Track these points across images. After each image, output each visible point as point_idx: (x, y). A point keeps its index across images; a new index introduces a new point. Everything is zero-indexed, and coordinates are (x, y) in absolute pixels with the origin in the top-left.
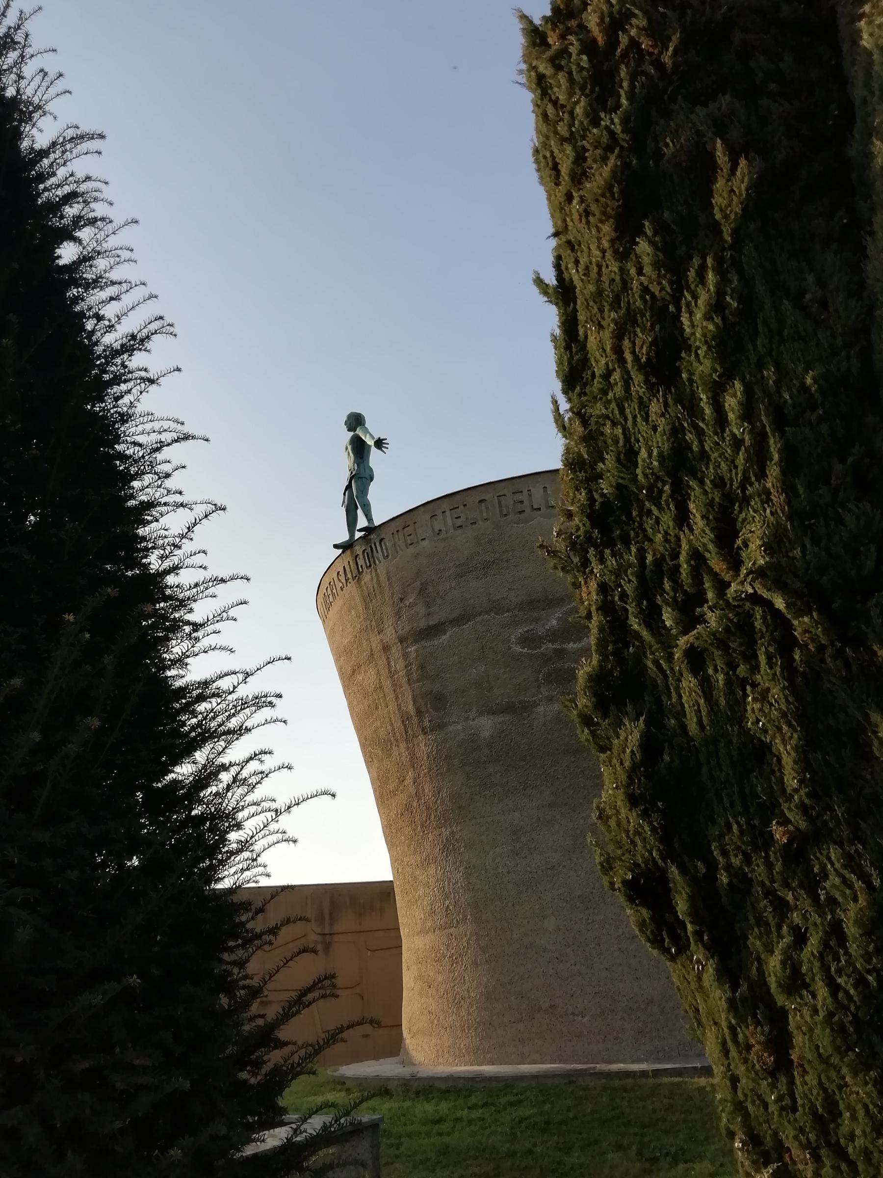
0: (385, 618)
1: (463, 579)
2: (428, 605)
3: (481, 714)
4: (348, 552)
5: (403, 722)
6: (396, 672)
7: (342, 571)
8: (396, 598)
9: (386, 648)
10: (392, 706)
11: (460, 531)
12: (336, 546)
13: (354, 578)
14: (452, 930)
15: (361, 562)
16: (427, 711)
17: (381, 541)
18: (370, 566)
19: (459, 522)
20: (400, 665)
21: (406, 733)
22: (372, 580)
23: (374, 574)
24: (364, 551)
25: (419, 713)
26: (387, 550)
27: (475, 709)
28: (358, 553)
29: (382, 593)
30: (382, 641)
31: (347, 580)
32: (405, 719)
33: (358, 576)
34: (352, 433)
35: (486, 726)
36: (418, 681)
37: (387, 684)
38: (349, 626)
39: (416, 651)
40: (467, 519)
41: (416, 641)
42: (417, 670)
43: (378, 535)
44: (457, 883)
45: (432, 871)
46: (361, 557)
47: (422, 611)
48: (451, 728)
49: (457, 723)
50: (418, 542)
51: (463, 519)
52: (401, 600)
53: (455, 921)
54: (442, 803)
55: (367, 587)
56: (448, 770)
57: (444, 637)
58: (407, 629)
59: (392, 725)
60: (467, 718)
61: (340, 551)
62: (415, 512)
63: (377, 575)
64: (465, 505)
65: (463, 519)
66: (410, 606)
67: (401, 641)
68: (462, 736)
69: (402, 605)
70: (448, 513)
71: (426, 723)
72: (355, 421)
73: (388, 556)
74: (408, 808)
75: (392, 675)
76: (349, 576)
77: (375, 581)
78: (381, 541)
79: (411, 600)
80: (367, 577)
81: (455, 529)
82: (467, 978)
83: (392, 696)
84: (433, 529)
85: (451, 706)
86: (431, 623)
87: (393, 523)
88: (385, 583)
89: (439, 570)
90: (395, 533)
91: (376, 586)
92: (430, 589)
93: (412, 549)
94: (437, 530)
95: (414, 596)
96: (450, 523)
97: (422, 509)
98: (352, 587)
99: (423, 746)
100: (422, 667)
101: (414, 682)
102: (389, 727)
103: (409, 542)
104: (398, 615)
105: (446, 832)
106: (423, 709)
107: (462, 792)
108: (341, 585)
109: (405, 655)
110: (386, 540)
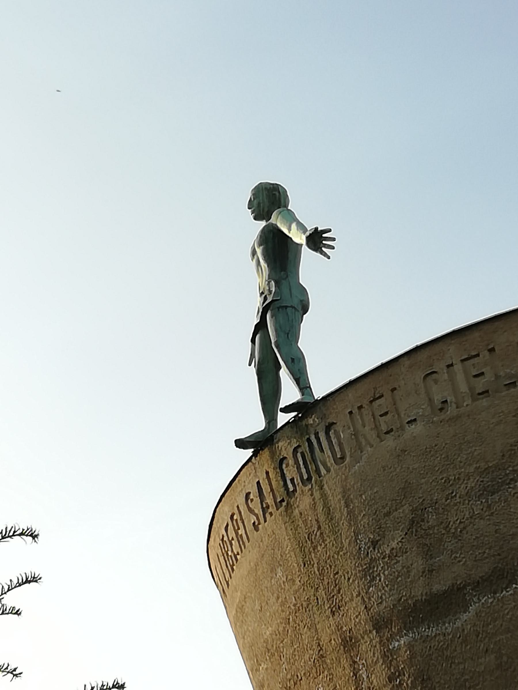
1: (496, 497)
2: (428, 552)
4: (266, 454)
7: (254, 491)
8: (364, 540)
9: (349, 643)
11: (484, 402)
12: (240, 444)
13: (278, 505)
15: (290, 472)
17: (328, 428)
18: (309, 479)
19: (480, 385)
24: (295, 450)
26: (340, 444)
28: (284, 454)
29: (334, 531)
30: (339, 628)
33: (286, 500)
34: (263, 223)
38: (273, 600)
39: (410, 646)
40: (497, 377)
41: (407, 627)
43: (323, 417)
46: (291, 462)
47: (418, 564)
50: (402, 428)
51: (489, 376)
52: (374, 544)
55: (305, 522)
57: (465, 617)
58: (389, 601)
61: (249, 452)
63: (324, 496)
64: (492, 350)
65: (489, 376)
67: (379, 624)
69: (376, 554)
70: (458, 367)
72: (269, 200)
73: (343, 458)
77: (320, 508)
78: (328, 428)
79: (394, 544)
80: (303, 502)
81: (474, 400)
84: (431, 400)
86: (436, 588)
87: (351, 394)
88: (340, 513)
89: (448, 480)
90: (355, 411)
91: (322, 518)
92: (432, 519)
93: (390, 442)
94: (437, 398)
95: (399, 534)
96: (463, 388)
97: (406, 362)
98: (275, 524)
104: (369, 574)
108: (253, 519)
109: (388, 656)
110: (339, 427)
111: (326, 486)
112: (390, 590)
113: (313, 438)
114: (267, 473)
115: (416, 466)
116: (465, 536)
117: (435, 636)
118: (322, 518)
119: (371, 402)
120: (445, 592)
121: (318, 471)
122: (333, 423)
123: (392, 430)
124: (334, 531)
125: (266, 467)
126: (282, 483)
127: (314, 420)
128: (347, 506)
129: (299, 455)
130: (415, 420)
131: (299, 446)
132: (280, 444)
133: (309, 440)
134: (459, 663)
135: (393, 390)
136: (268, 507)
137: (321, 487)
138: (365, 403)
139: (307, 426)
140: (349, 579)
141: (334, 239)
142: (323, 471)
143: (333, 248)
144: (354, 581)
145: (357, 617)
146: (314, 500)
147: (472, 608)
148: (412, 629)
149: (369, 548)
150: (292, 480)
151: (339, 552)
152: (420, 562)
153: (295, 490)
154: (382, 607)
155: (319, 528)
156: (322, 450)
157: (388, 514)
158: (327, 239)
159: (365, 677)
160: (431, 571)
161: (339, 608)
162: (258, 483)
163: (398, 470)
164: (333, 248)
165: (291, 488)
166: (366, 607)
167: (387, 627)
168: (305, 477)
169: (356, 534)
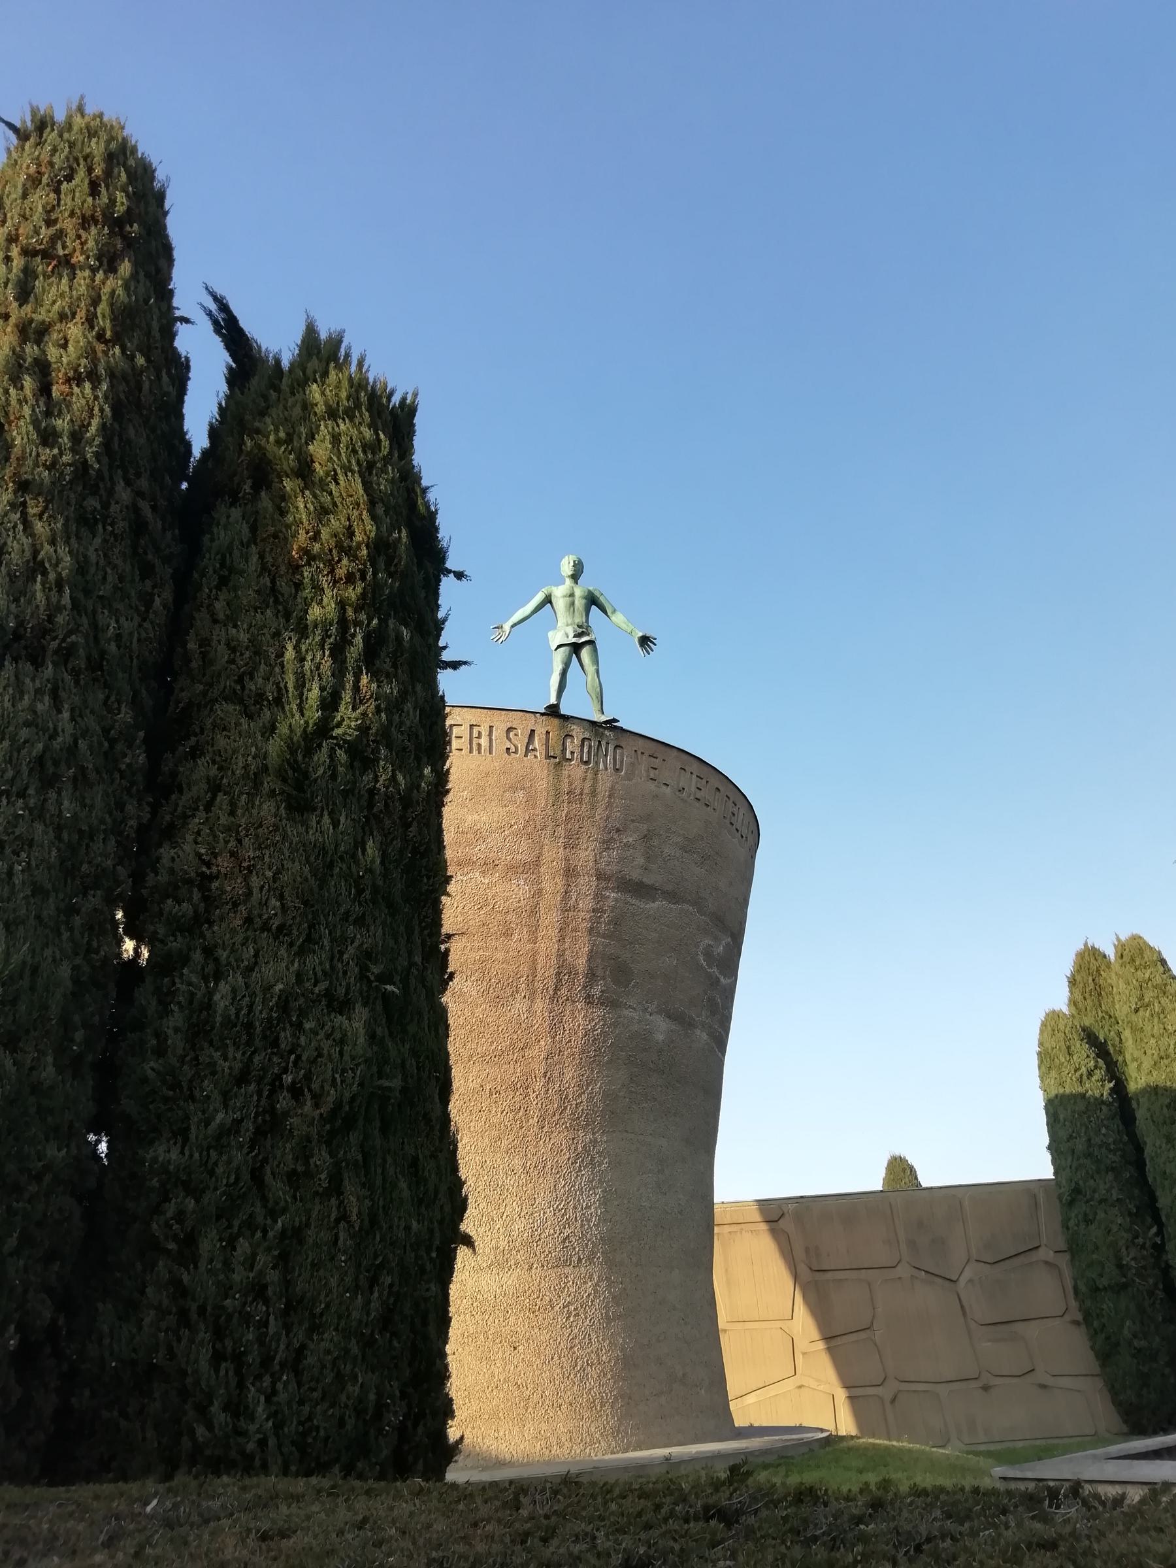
2: (648, 859)
3: (659, 1012)
4: (556, 721)
5: (558, 974)
8: (612, 823)
9: (570, 873)
10: (547, 945)
13: (548, 757)
14: (568, 1270)
15: (572, 746)
16: (604, 978)
20: (586, 904)
21: (556, 990)
22: (584, 780)
23: (590, 775)
25: (591, 975)
28: (574, 734)
29: (593, 805)
30: (567, 859)
32: (564, 970)
33: (558, 760)
35: (661, 1028)
36: (604, 936)
37: (550, 918)
39: (616, 900)
41: (618, 888)
42: (609, 922)
44: (588, 1207)
45: (548, 1183)
47: (640, 860)
48: (626, 1012)
52: (618, 830)
53: (575, 1258)
54: (590, 1099)
55: (570, 784)
56: (610, 1061)
59: (533, 968)
62: (667, 749)
63: (595, 779)
66: (627, 845)
67: (601, 876)
68: (636, 1027)
71: (596, 991)
74: (522, 1087)
76: (537, 743)
77: (588, 784)
78: (617, 747)
79: (631, 840)
80: (575, 770)
82: (594, 1337)
83: (554, 933)
85: (634, 986)
87: (641, 741)
91: (586, 791)
93: (652, 786)
94: (681, 785)
95: (635, 836)
97: (675, 752)
98: (538, 766)
99: (580, 1020)
100: (616, 922)
101: (599, 935)
102: (524, 970)
103: (652, 776)
104: (607, 844)
105: (584, 1137)
106: (599, 972)
107: (621, 1094)
109: (599, 897)
113: (603, 744)
114: (548, 733)
118: (586, 791)
121: (597, 763)
124: (593, 805)
125: (549, 728)
128: (610, 797)
136: (534, 750)
138: (647, 754)
150: (572, 753)
153: (570, 760)
155: (581, 794)
156: (606, 755)
157: (633, 821)
162: (533, 731)
165: (568, 756)
169: (608, 818)
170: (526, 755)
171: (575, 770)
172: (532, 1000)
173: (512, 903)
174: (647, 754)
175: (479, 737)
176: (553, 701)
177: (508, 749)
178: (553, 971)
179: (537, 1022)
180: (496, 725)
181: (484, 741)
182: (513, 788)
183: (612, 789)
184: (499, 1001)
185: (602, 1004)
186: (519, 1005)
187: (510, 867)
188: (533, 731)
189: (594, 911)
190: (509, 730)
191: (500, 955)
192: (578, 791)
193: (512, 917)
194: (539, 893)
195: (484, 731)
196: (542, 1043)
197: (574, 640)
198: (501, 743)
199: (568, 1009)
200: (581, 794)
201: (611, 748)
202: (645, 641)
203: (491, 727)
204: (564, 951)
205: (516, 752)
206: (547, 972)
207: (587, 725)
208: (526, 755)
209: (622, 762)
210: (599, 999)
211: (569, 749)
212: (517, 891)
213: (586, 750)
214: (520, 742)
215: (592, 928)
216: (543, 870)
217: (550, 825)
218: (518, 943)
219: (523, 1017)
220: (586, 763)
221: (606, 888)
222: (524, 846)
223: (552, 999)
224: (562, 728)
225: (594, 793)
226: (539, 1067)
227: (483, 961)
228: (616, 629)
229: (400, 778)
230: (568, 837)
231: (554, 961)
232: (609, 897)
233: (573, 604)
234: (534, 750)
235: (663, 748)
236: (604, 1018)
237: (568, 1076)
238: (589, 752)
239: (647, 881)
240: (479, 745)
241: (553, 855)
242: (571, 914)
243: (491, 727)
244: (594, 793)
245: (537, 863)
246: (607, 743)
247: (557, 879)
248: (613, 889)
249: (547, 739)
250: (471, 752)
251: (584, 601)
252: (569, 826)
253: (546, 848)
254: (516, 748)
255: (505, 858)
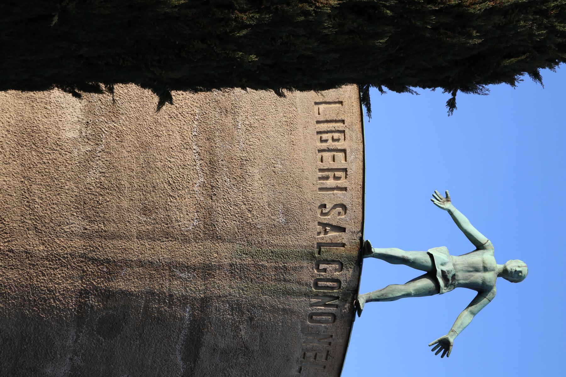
0: (243, 285)
4: (355, 253)
5: (108, 261)
6: (173, 276)
9: (207, 270)
10: (137, 249)
13: (320, 245)
16: (105, 308)
18: (316, 285)
20: (177, 288)
21: (93, 260)
22: (299, 283)
23: (304, 289)
26: (319, 322)
27: (82, 364)
28: (344, 272)
29: (275, 293)
30: (220, 267)
31: (324, 225)
32: (112, 267)
33: (317, 256)
36: (146, 307)
37: (163, 251)
39: (182, 319)
42: (159, 312)
43: (342, 317)
47: (222, 344)
48: (72, 332)
49: (76, 341)
52: (251, 319)
55: (295, 269)
56: (24, 316)
57: (179, 358)
59: (114, 236)
60: (75, 353)
63: (300, 294)
66: (237, 329)
67: (205, 302)
69: (245, 317)
71: (92, 301)
75: (172, 268)
77: (295, 287)
78: (334, 316)
79: (243, 333)
80: (308, 273)
83: (148, 256)
85: (98, 340)
86: (204, 349)
87: (341, 341)
91: (288, 286)
92: (241, 360)
93: (298, 354)
98: (310, 235)
102: (111, 228)
103: (308, 354)
104: (237, 308)
108: (329, 206)
109: (184, 300)
111: (303, 299)
112: (219, 320)
113: (336, 302)
114: (343, 245)
115: (275, 364)
116: (221, 374)
117: (178, 337)
118: (288, 286)
119: (328, 351)
120: (198, 353)
121: (316, 296)
122: (334, 322)
123: (304, 358)
124: (275, 293)
125: (348, 246)
126: (329, 258)
127: (346, 309)
128: (284, 310)
129: (335, 284)
130: (300, 372)
131: (340, 288)
132: (351, 271)
133: (337, 298)
134: (156, 345)
135: (325, 367)
137: (306, 295)
138: (330, 348)
139: (346, 301)
140: (243, 290)
141: (436, 354)
142: (314, 300)
143: (433, 350)
144: (239, 293)
145: (218, 287)
146: (303, 285)
147: (181, 363)
148: (190, 324)
149: (251, 314)
150: (325, 270)
151: (262, 289)
152: (223, 346)
153: (318, 269)
154: (213, 309)
155: (285, 280)
156: (325, 305)
157: (261, 335)
158: (440, 350)
159: (181, 275)
160: (214, 350)
161: (232, 273)
162: (343, 230)
163: (280, 353)
164: (433, 350)
165: (322, 266)
166: (220, 296)
167: (201, 307)
168: (320, 283)
170: (320, 224)
171: (308, 273)
172: (82, 236)
173: (175, 214)
174: (330, 348)
175: (336, 178)
176: (376, 250)
177: (324, 206)
178: (110, 256)
179: (61, 241)
180: (348, 194)
181: (331, 183)
182: (287, 212)
183: (292, 312)
184: (80, 204)
185: (80, 306)
186: (77, 224)
187: (210, 211)
188: (343, 230)
189: (171, 296)
190: (344, 207)
191: (125, 204)
192: (288, 277)
193: (162, 214)
194: (186, 240)
195: (342, 183)
196: (41, 248)
197: (439, 269)
198: (330, 199)
199: (74, 273)
200: (285, 280)
201: (332, 310)
202: (444, 346)
203: (345, 189)
204: (131, 267)
205: (322, 214)
206: (110, 250)
207: (354, 284)
208: (320, 224)
209: (319, 322)
210: (85, 304)
211: (329, 267)
212: (187, 219)
213: (329, 284)
214: (333, 218)
215: (153, 294)
216: (209, 243)
217: (253, 249)
218: (136, 221)
219: (66, 228)
220: (316, 285)
221: (193, 309)
222: (232, 225)
223: (84, 256)
224: (349, 259)
225: (287, 293)
226: (18, 245)
227: (119, 188)
228: (451, 311)
229: (244, 32)
230: (242, 268)
231: (120, 256)
232: (185, 311)
233: (477, 270)
234: (326, 232)
235: (336, 366)
236: (67, 309)
237: (9, 274)
238: (327, 287)
239: (203, 351)
240: (327, 178)
241: (224, 253)
242: (167, 273)
243: (345, 189)
244: (287, 293)
245: (216, 238)
246: (337, 306)
247: (200, 258)
248: (193, 315)
249: (337, 245)
250: (321, 170)
251: (480, 281)
252: (252, 269)
253: (230, 246)
254: (326, 214)
255: (218, 205)
